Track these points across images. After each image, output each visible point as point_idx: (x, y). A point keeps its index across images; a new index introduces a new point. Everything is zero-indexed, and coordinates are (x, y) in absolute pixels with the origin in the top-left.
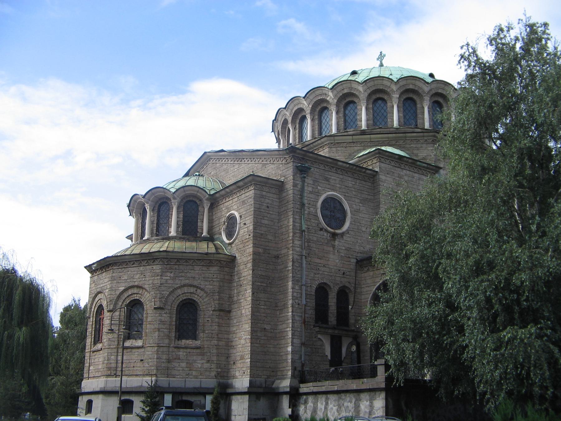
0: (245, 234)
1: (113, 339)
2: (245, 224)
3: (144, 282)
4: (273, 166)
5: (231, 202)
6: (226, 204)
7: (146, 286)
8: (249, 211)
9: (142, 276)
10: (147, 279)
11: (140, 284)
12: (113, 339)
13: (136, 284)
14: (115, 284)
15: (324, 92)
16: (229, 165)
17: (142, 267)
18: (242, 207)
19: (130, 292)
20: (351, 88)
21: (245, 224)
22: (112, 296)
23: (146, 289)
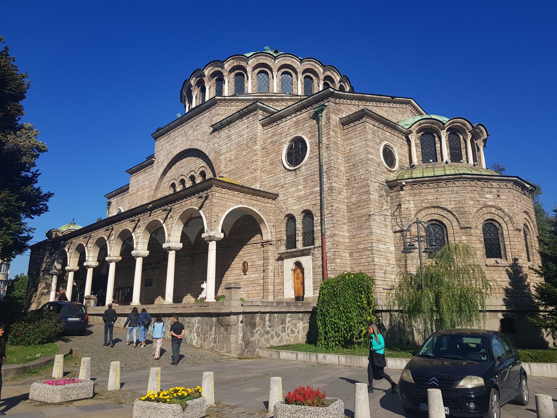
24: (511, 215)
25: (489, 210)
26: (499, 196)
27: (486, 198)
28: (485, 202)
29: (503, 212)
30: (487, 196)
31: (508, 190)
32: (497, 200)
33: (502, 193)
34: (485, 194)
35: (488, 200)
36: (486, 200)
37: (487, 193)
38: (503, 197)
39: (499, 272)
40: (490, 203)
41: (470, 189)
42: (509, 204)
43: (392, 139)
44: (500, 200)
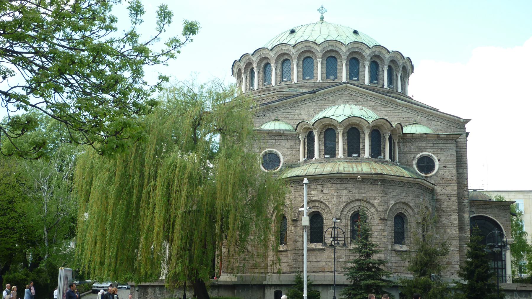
0: (446, 174)
1: (388, 243)
2: (445, 167)
3: (409, 200)
4: (442, 125)
5: (424, 145)
6: (417, 145)
7: (411, 204)
8: (450, 158)
9: (407, 196)
10: (411, 198)
11: (406, 201)
12: (388, 243)
13: (403, 201)
14: (387, 198)
15: (362, 47)
16: (379, 104)
17: (406, 188)
18: (441, 153)
19: (398, 206)
20: (380, 52)
21: (445, 167)
22: (385, 207)
23: (410, 207)
24: (330, 206)
25: (314, 204)
26: (322, 191)
27: (312, 194)
28: (310, 197)
29: (325, 204)
30: (313, 192)
31: (331, 185)
32: (321, 195)
33: (325, 189)
34: (311, 191)
35: (313, 196)
36: (311, 196)
37: (313, 190)
38: (325, 192)
39: (315, 254)
40: (314, 198)
41: (300, 188)
42: (330, 197)
43: (279, 144)
44: (323, 195)
